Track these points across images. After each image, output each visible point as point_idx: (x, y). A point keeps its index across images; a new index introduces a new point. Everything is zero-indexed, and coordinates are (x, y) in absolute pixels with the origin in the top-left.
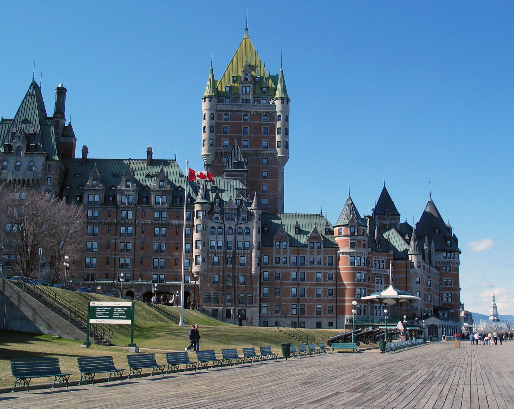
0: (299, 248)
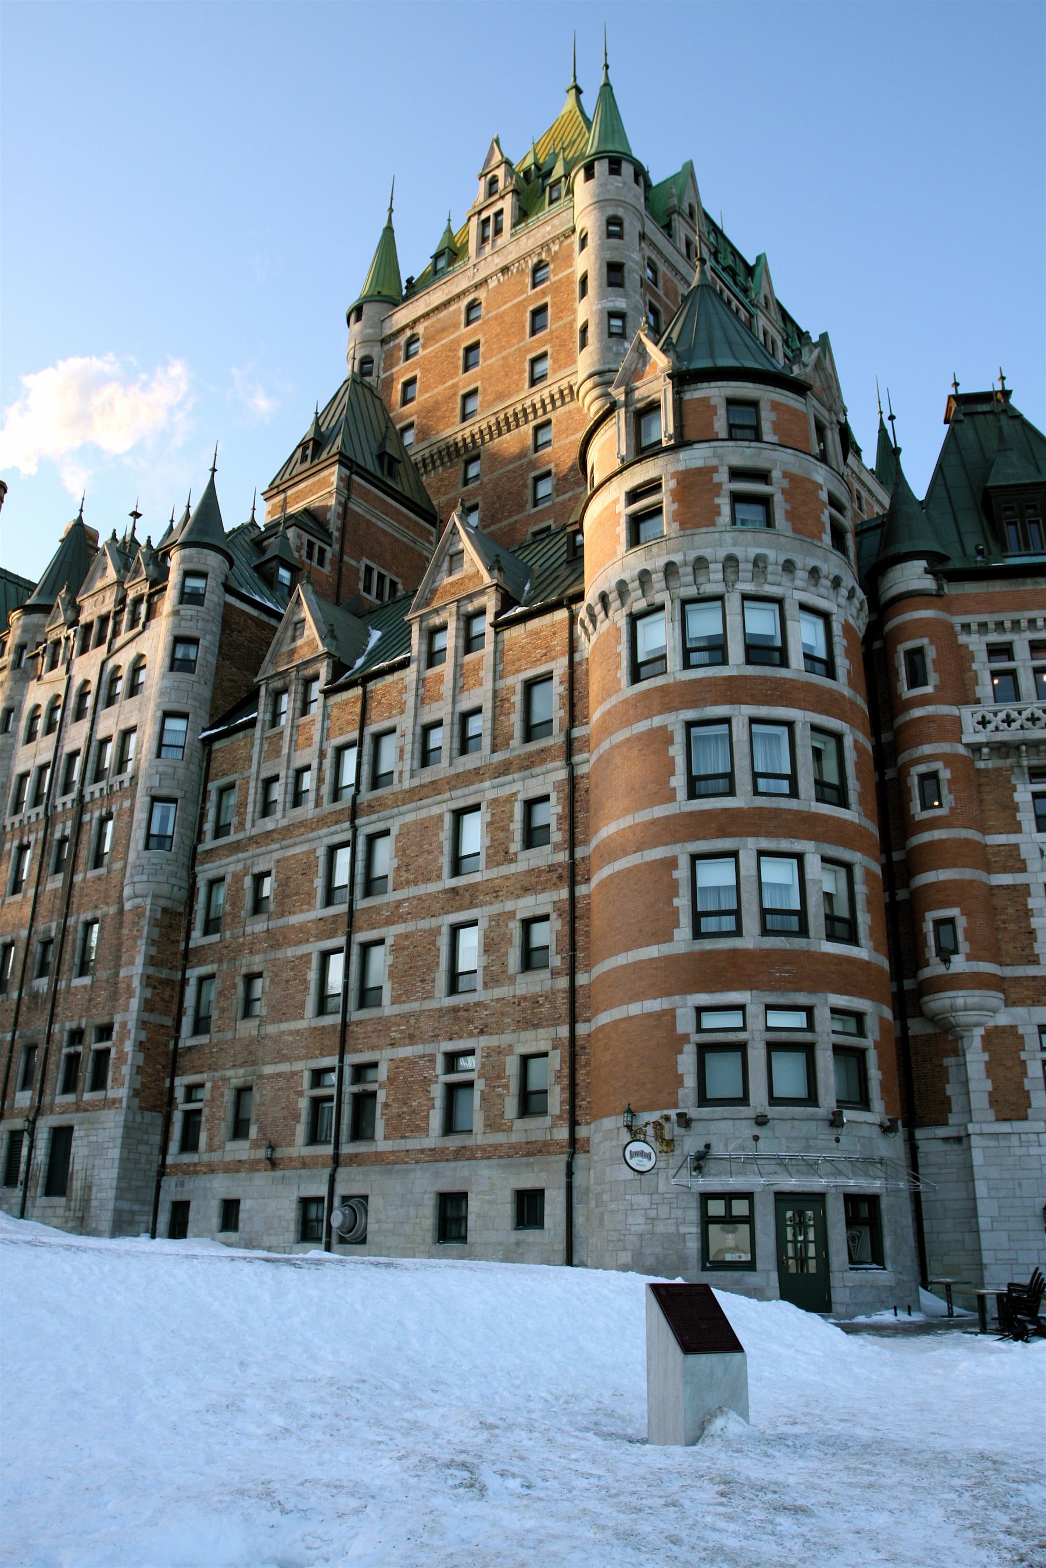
0: (371, 686)
